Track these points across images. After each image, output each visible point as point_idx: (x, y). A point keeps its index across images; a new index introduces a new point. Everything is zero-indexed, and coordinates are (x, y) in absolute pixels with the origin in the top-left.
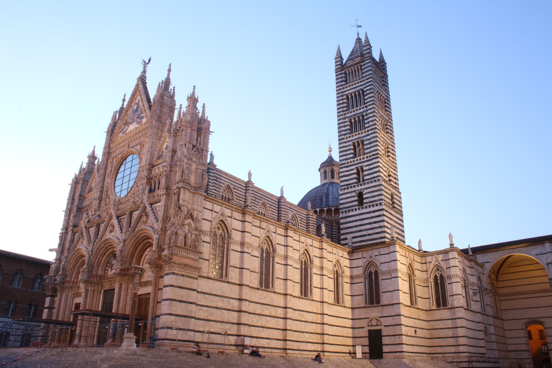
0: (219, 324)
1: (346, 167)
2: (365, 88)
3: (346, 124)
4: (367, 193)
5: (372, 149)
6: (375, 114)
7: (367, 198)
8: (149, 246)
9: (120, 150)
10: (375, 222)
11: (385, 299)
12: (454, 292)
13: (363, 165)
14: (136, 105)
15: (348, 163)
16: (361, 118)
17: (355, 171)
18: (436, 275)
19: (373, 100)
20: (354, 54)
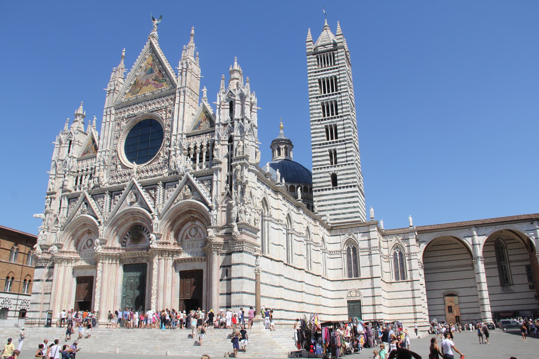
0: (267, 299)
1: (319, 148)
2: (339, 75)
3: (319, 107)
4: (341, 175)
5: (346, 134)
6: (348, 101)
7: (341, 179)
8: (189, 221)
9: (131, 113)
10: (349, 203)
11: (364, 272)
12: (413, 267)
13: (336, 149)
14: (150, 66)
15: (320, 145)
16: (334, 103)
17: (328, 153)
18: (395, 252)
19: (347, 88)
20: (324, 41)
